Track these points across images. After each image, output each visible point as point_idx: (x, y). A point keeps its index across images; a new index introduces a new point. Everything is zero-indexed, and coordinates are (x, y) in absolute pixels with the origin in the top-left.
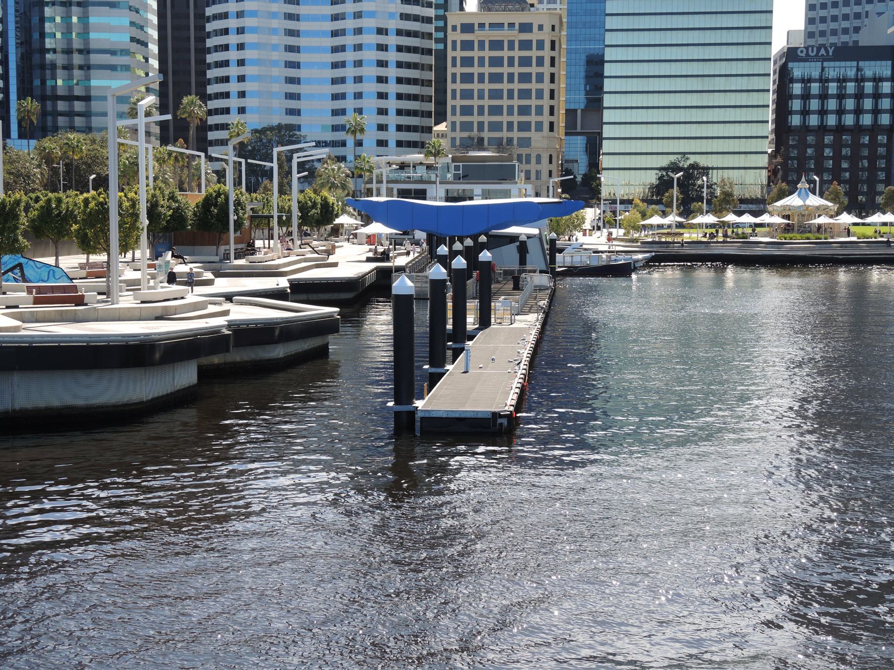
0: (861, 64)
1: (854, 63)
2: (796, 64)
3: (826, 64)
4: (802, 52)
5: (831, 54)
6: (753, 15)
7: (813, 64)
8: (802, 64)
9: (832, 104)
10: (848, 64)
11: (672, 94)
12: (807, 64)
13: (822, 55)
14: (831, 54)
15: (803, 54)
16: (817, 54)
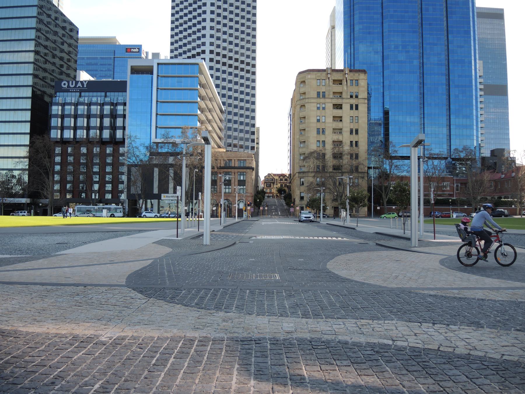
0: (108, 94)
1: (103, 94)
2: (61, 94)
3: (83, 94)
4: (65, 84)
5: (85, 86)
6: (20, 54)
7: (74, 94)
8: (66, 94)
9: (82, 122)
10: (99, 94)
11: (7, 124)
12: (70, 94)
13: (79, 87)
14: (85, 86)
15: (66, 86)
16: (75, 87)
